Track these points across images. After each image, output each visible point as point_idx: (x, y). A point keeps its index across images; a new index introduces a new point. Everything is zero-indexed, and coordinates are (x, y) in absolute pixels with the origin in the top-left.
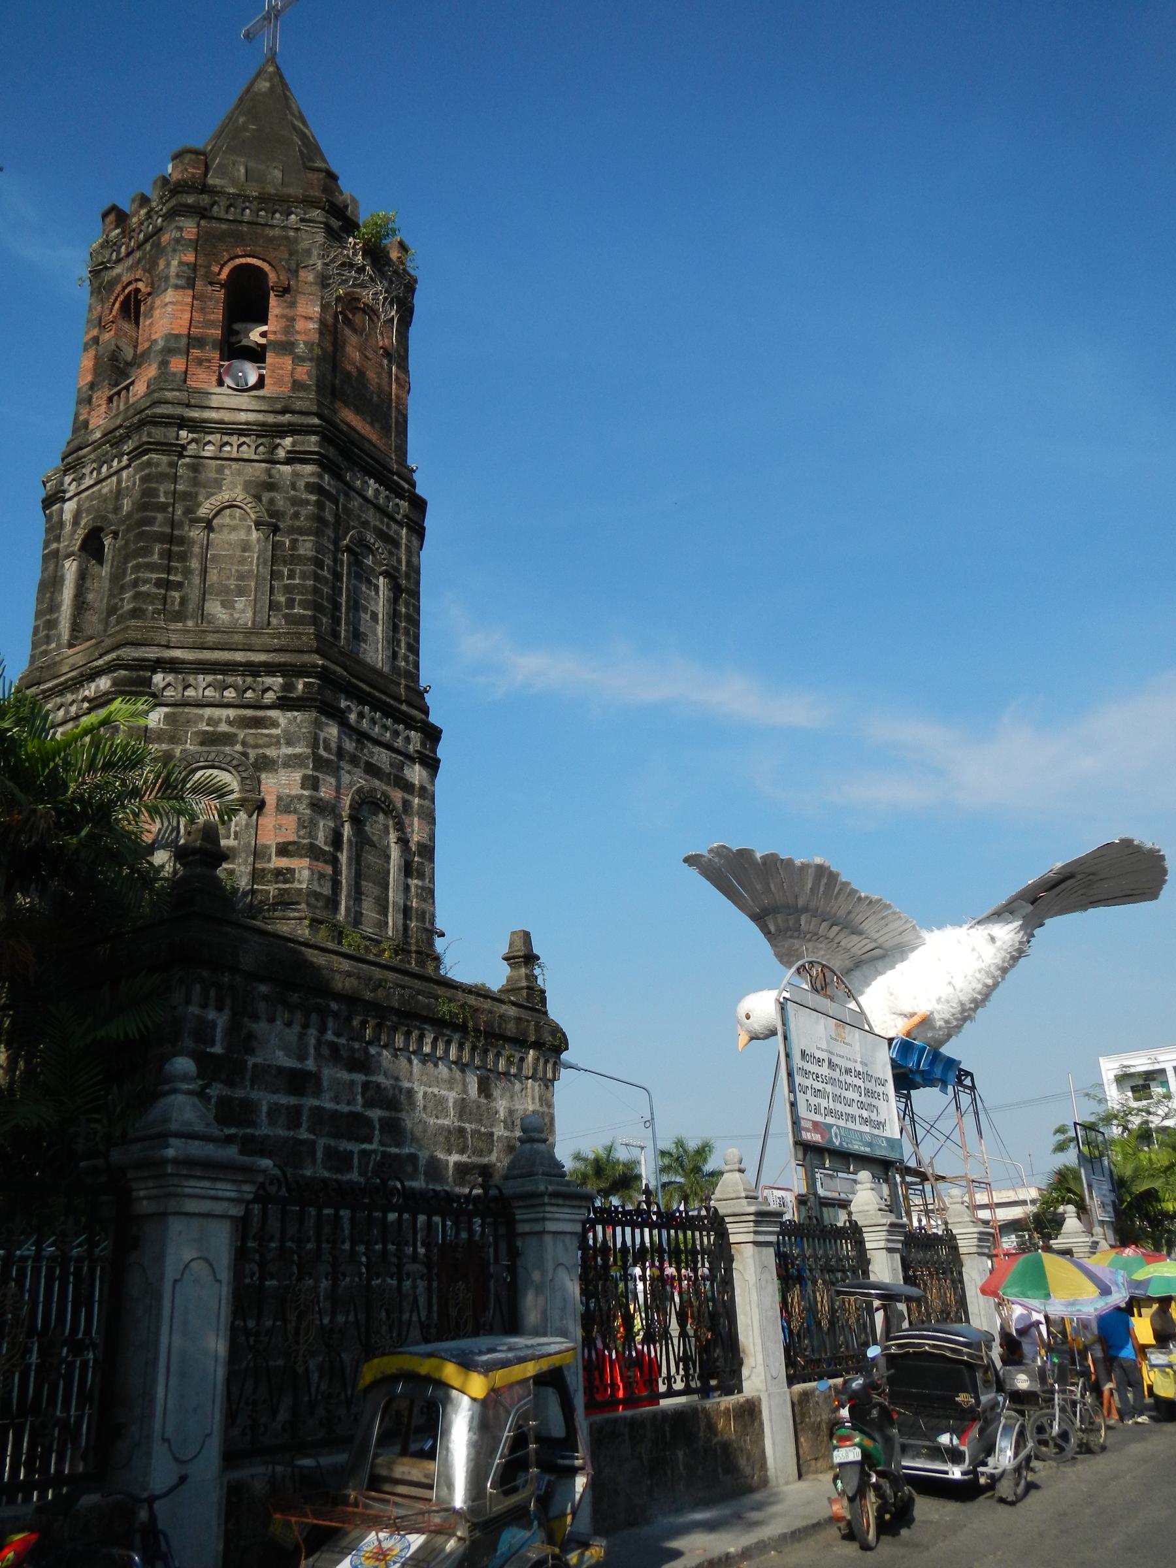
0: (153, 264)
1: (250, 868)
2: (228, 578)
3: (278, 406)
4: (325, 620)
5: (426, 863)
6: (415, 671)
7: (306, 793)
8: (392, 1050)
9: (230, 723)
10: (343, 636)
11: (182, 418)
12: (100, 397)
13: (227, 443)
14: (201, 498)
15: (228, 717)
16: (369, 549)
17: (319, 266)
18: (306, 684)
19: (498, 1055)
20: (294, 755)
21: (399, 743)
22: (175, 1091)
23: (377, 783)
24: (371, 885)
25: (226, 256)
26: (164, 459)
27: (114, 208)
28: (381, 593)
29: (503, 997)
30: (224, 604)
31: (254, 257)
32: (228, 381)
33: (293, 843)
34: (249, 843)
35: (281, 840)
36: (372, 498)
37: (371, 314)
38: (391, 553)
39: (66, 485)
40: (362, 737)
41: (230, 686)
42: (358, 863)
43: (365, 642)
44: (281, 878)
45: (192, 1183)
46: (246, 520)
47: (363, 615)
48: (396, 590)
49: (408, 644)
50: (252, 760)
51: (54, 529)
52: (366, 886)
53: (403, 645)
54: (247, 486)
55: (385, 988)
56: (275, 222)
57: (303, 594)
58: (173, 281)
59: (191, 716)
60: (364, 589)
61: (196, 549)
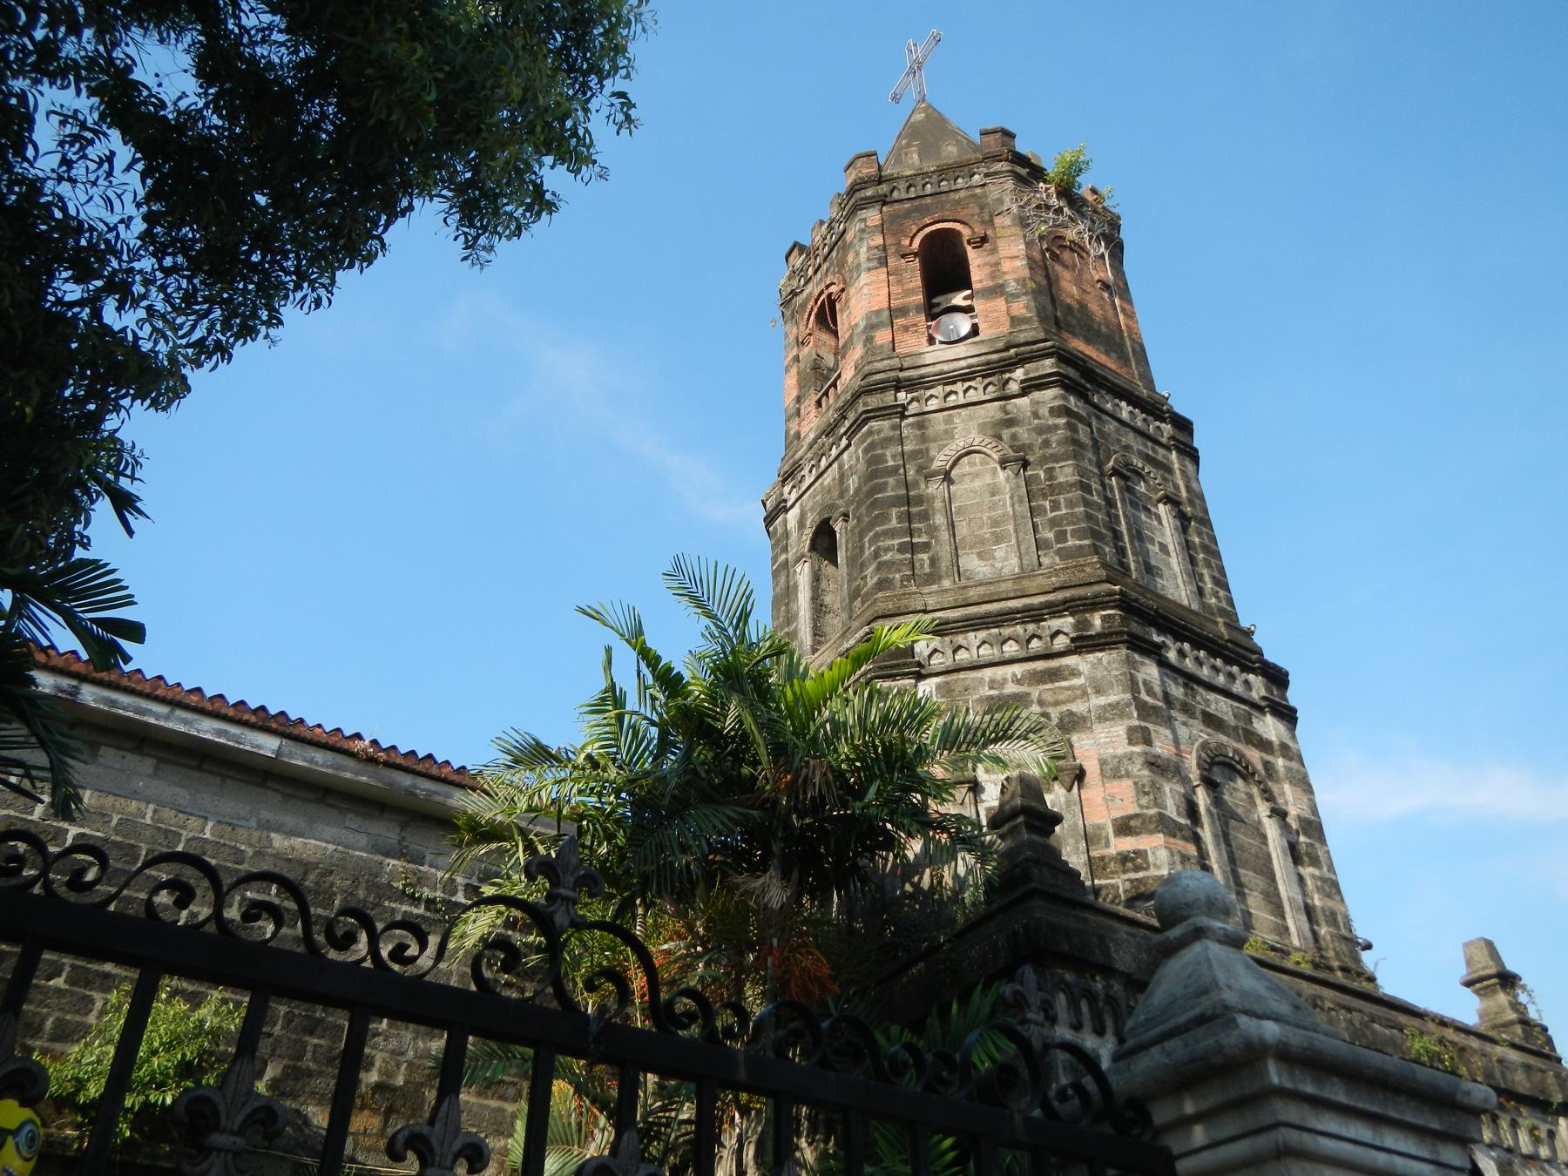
0: (842, 263)
1: (1084, 858)
2: (981, 528)
3: (1000, 345)
4: (1107, 549)
5: (1317, 845)
6: (1229, 609)
7: (1138, 749)
9: (1018, 682)
10: (1133, 567)
11: (898, 380)
12: (809, 405)
13: (951, 393)
14: (933, 453)
15: (1014, 675)
16: (1139, 474)
17: (1015, 209)
18: (1104, 618)
19: (1514, 1125)
20: (1109, 705)
21: (1237, 688)
22: (1199, 933)
23: (1223, 739)
24: (1251, 874)
25: (915, 229)
26: (886, 424)
27: (795, 245)
28: (1165, 522)
29: (1491, 1033)
30: (980, 556)
32: (939, 337)
33: (1136, 816)
34: (1076, 825)
35: (1118, 814)
36: (1128, 420)
38: (1165, 479)
39: (786, 496)
40: (1190, 680)
41: (1009, 639)
42: (1228, 844)
43: (1161, 577)
44: (1130, 865)
45: (1331, 1123)
46: (987, 463)
47: (1150, 547)
48: (1183, 520)
49: (1214, 578)
50: (1055, 721)
51: (780, 542)
52: (1246, 875)
53: (1207, 579)
54: (982, 428)
55: (1322, 1009)
56: (958, 186)
57: (1074, 524)
58: (865, 265)
59: (968, 682)
60: (1143, 517)
61: (938, 504)
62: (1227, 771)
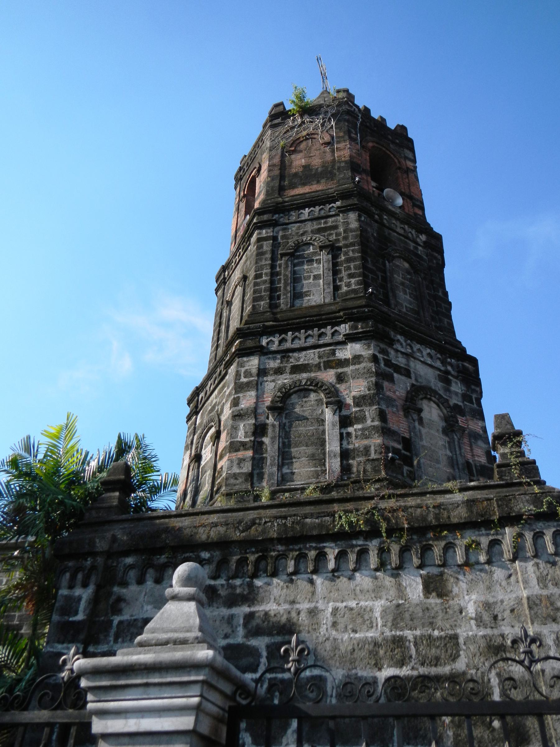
8: (285, 577)
21: (327, 339)
40: (285, 354)
52: (297, 451)
62: (302, 394)
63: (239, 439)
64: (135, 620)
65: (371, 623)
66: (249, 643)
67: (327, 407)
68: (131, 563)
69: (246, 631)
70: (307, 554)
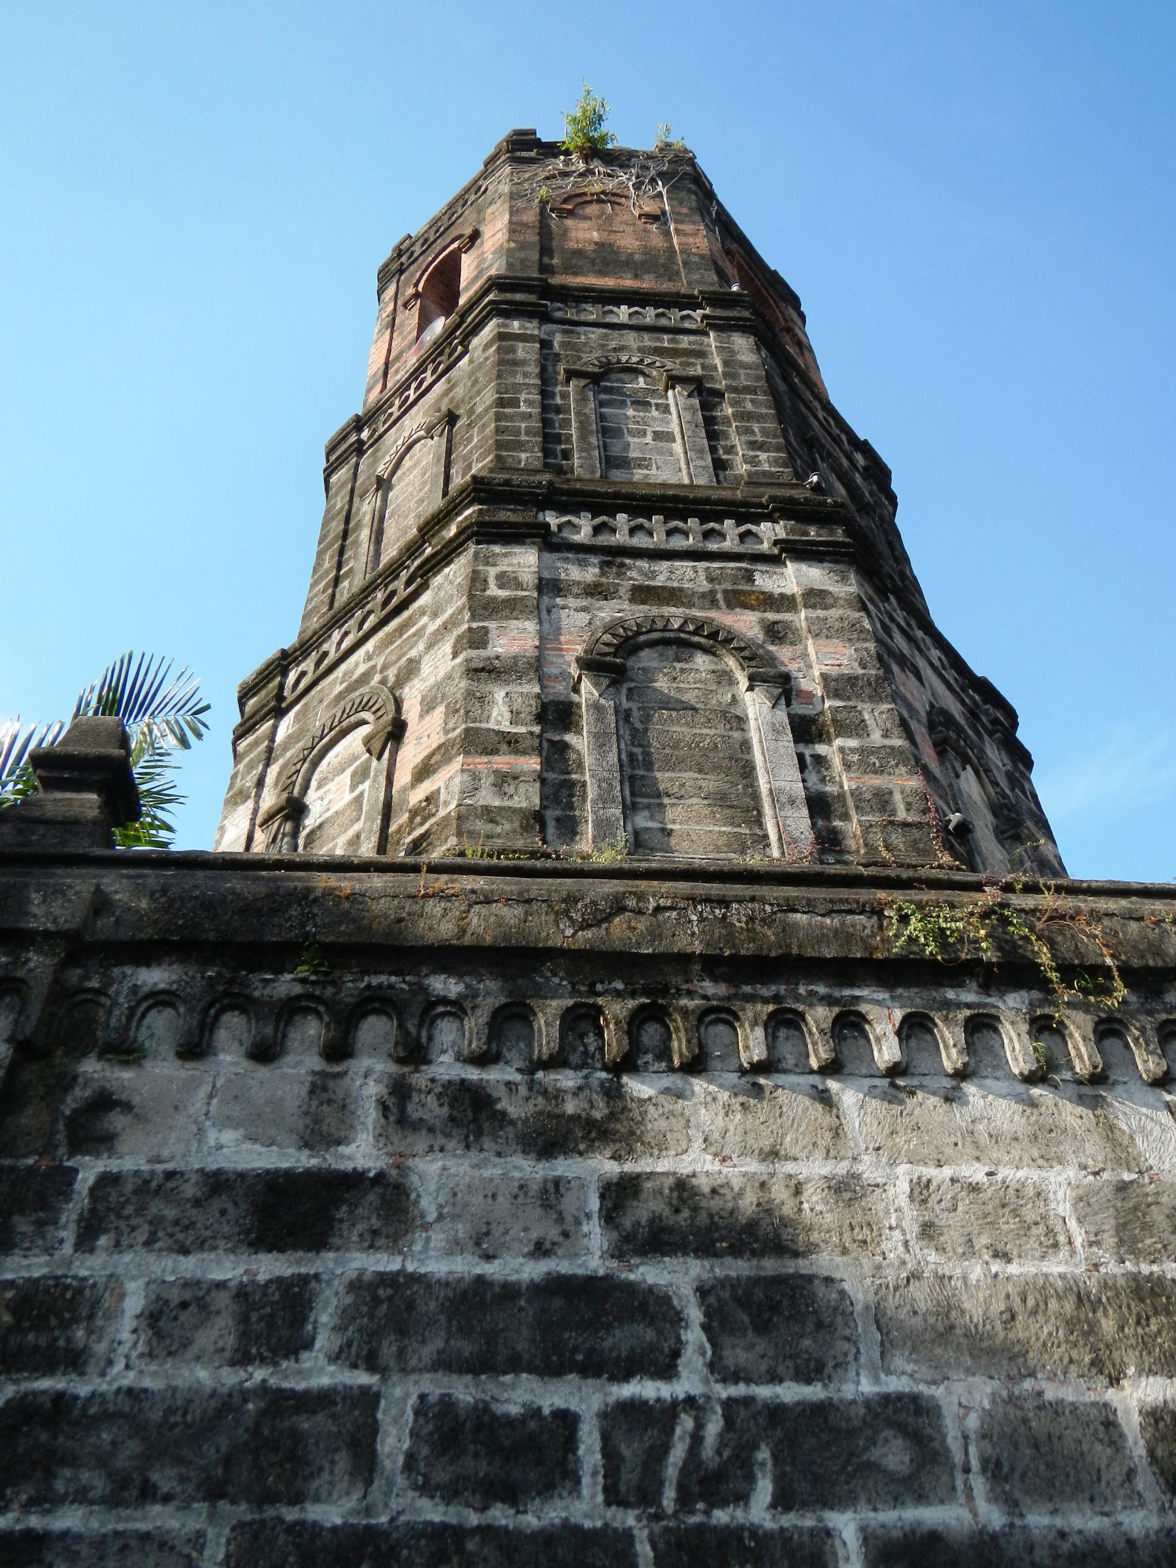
8: (733, 1077)
21: (729, 544)
31: (444, 249)
37: (613, 199)
40: (614, 556)
52: (671, 779)
62: (671, 651)
63: (492, 725)
64: (170, 1175)
65: (1050, 1232)
66: (632, 1277)
67: (750, 688)
68: (162, 986)
69: (615, 1235)
70: (801, 1016)
